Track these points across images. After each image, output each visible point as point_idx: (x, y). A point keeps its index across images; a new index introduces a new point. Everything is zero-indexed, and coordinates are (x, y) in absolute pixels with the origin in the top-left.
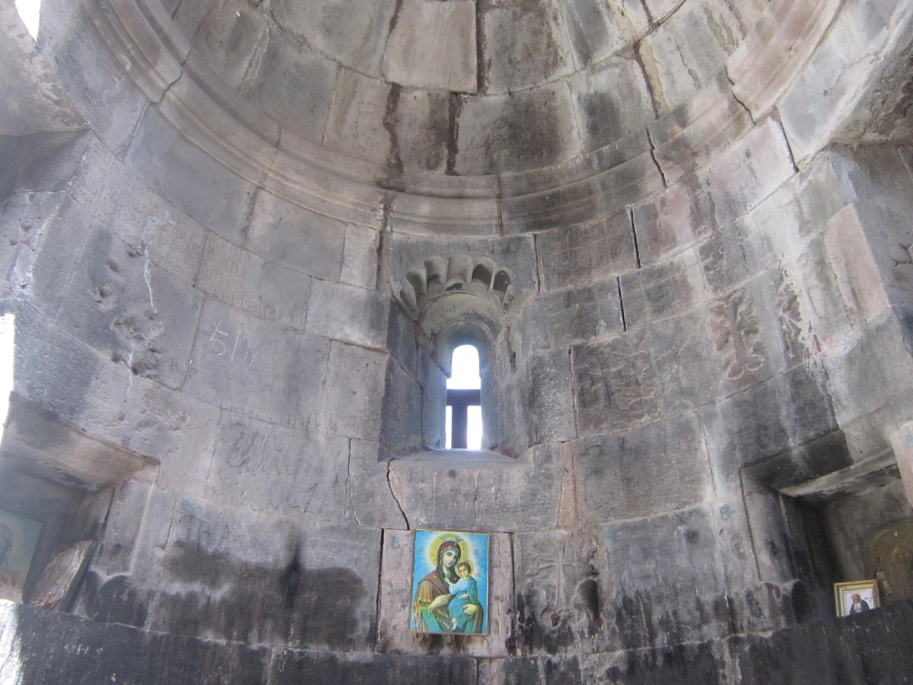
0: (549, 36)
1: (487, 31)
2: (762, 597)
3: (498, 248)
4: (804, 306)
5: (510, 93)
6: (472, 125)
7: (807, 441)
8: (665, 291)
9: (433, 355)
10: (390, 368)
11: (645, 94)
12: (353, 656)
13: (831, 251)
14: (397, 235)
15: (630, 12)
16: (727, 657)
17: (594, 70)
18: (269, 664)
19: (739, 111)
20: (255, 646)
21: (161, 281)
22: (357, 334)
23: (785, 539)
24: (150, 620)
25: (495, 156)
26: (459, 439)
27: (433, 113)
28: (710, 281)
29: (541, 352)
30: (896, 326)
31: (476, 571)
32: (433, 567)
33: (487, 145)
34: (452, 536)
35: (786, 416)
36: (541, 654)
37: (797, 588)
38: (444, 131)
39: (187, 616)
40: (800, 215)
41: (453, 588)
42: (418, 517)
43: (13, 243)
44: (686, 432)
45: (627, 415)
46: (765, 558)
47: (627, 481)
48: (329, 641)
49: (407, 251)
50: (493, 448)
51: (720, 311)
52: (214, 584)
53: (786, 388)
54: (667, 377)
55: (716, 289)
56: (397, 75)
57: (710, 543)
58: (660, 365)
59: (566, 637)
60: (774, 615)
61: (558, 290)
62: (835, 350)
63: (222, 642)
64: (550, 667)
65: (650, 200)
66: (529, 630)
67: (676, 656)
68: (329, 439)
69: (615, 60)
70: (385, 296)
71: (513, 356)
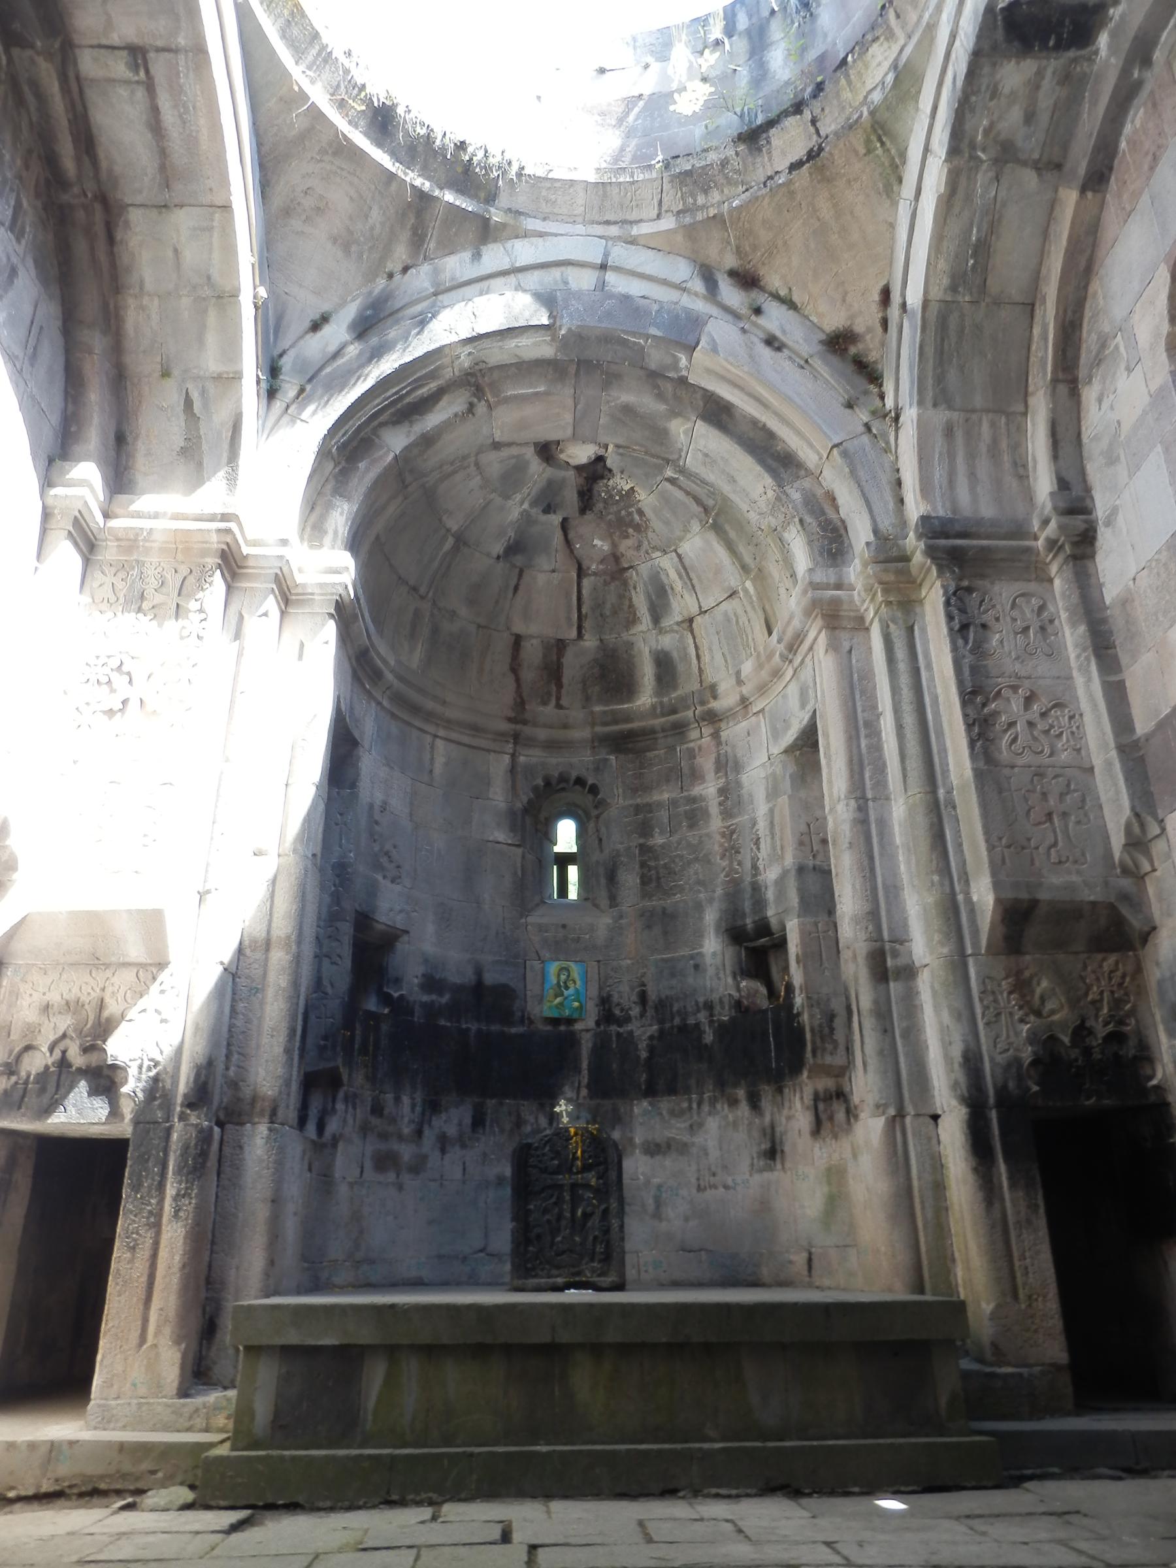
0: (630, 599)
1: (584, 592)
2: (726, 1000)
3: (591, 766)
4: (762, 846)
5: (601, 640)
6: (573, 666)
7: (754, 922)
8: (695, 815)
10: (523, 857)
11: (694, 661)
12: (514, 1030)
14: (522, 759)
15: (686, 596)
16: (707, 1029)
17: (661, 631)
19: (744, 702)
20: (464, 1026)
22: (500, 836)
24: (416, 1014)
25: (589, 691)
27: (545, 656)
28: (721, 813)
29: (620, 847)
30: (793, 872)
31: (578, 983)
32: (555, 982)
33: (584, 682)
34: (564, 964)
35: (747, 906)
36: (614, 1028)
38: (553, 672)
39: (431, 1011)
40: (767, 789)
41: (566, 993)
42: (546, 954)
43: (337, 824)
44: (699, 907)
46: (730, 980)
47: (665, 933)
50: (586, 899)
51: (723, 835)
52: (441, 994)
53: (749, 889)
54: (692, 871)
55: (723, 819)
56: (519, 627)
57: (705, 971)
58: (689, 863)
59: (628, 1019)
60: (730, 1009)
61: (631, 802)
62: (770, 875)
63: (448, 1024)
65: (691, 745)
66: (608, 1013)
67: (684, 1029)
69: (676, 628)
70: (519, 805)
71: (600, 840)
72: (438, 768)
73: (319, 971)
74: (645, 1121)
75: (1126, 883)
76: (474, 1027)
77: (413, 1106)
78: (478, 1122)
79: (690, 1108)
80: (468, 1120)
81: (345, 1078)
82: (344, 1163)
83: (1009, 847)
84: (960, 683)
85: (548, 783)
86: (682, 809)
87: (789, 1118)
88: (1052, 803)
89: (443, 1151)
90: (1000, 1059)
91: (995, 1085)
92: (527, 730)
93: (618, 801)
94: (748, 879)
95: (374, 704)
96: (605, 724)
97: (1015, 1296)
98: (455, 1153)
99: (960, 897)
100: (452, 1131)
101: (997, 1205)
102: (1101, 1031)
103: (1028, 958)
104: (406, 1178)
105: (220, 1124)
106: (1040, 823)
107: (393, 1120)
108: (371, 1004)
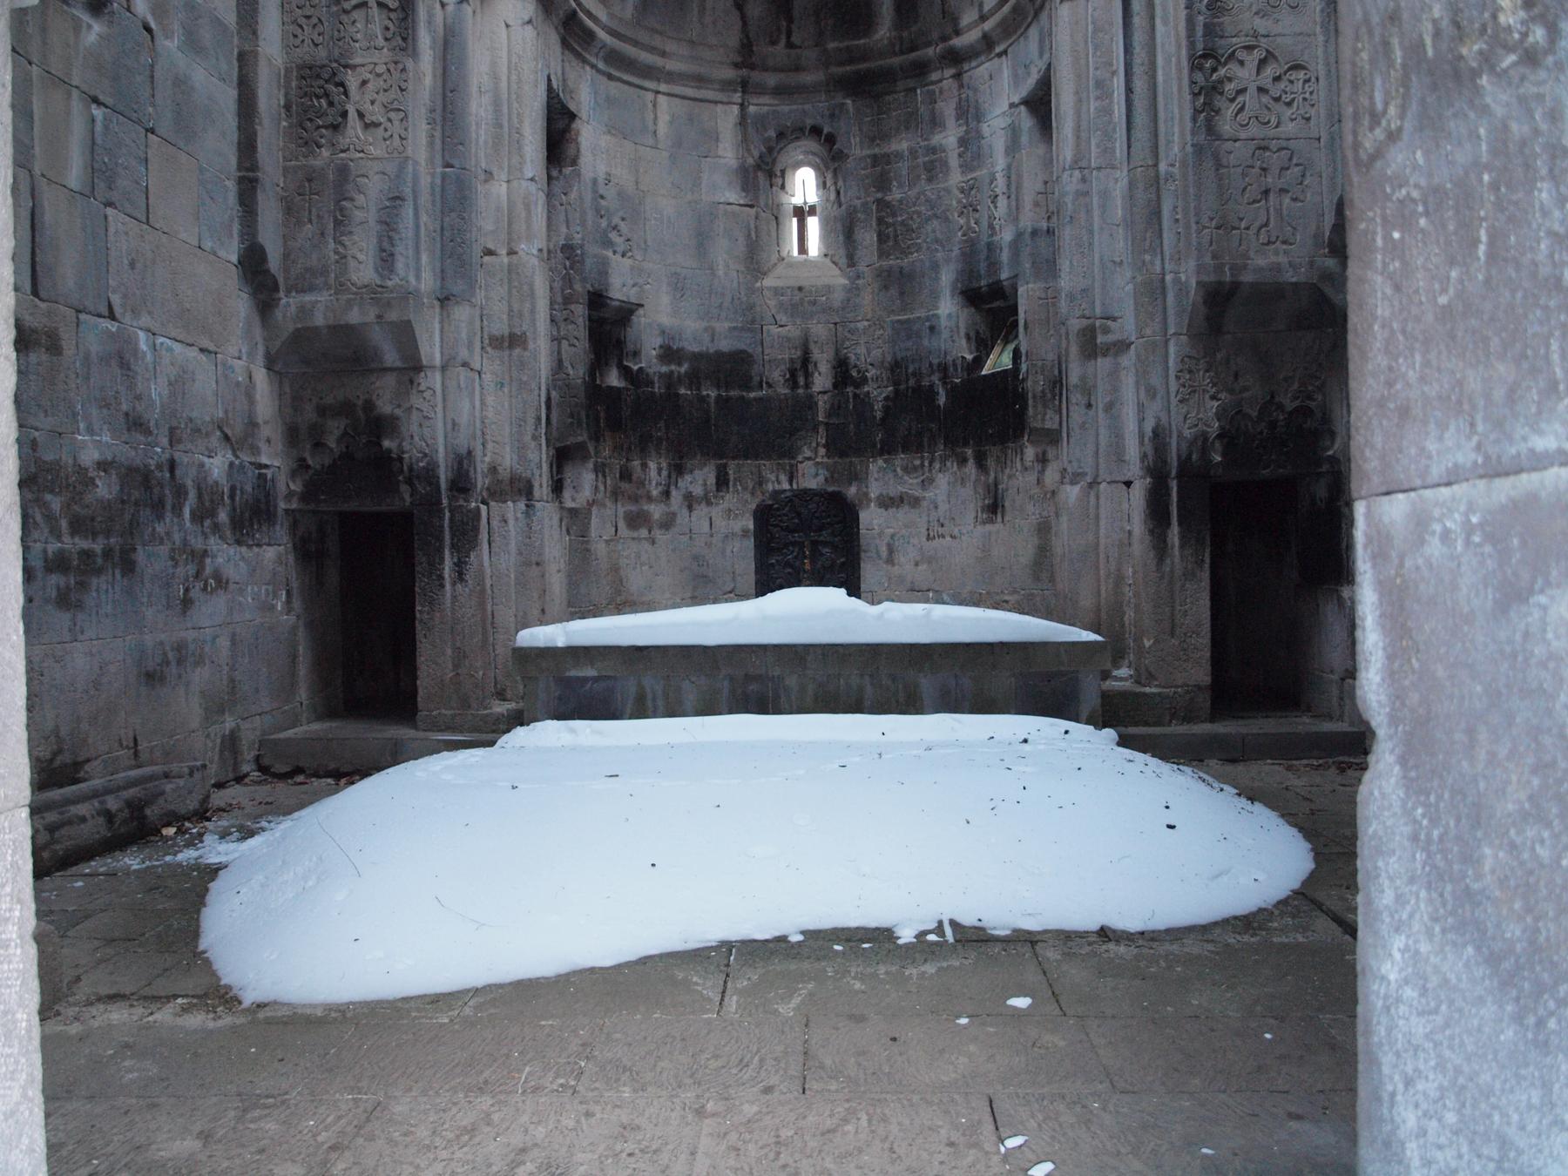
2: (959, 362)
8: (934, 167)
9: (783, 187)
12: (752, 395)
13: (1013, 177)
14: (752, 109)
18: (712, 400)
21: (621, 194)
22: (733, 196)
23: (978, 333)
29: (858, 203)
30: (1027, 236)
35: (983, 266)
37: (975, 359)
42: (782, 318)
44: (935, 267)
45: (905, 253)
46: (964, 342)
47: (902, 294)
48: (740, 387)
49: (761, 122)
52: (680, 364)
54: (929, 228)
57: (940, 333)
58: (928, 219)
59: (864, 380)
64: (856, 396)
67: (918, 389)
68: (726, 274)
70: (750, 161)
72: (662, 128)
73: (559, 353)
74: (879, 478)
75: (1331, 263)
76: (712, 393)
77: (660, 470)
78: (722, 482)
79: (922, 465)
80: (712, 480)
81: (591, 450)
82: (600, 526)
83: (1218, 228)
84: (1192, 44)
85: (781, 135)
86: (919, 160)
87: (1010, 477)
88: (1270, 180)
89: (690, 508)
90: (1187, 433)
91: (1179, 456)
92: (756, 76)
93: (857, 149)
94: (985, 239)
95: (588, 68)
96: (841, 64)
97: (1172, 634)
98: (701, 511)
99: (1168, 278)
100: (698, 490)
101: (1168, 561)
102: (1290, 405)
103: (1228, 337)
104: (657, 533)
106: (1255, 202)
107: (642, 484)
108: (614, 379)
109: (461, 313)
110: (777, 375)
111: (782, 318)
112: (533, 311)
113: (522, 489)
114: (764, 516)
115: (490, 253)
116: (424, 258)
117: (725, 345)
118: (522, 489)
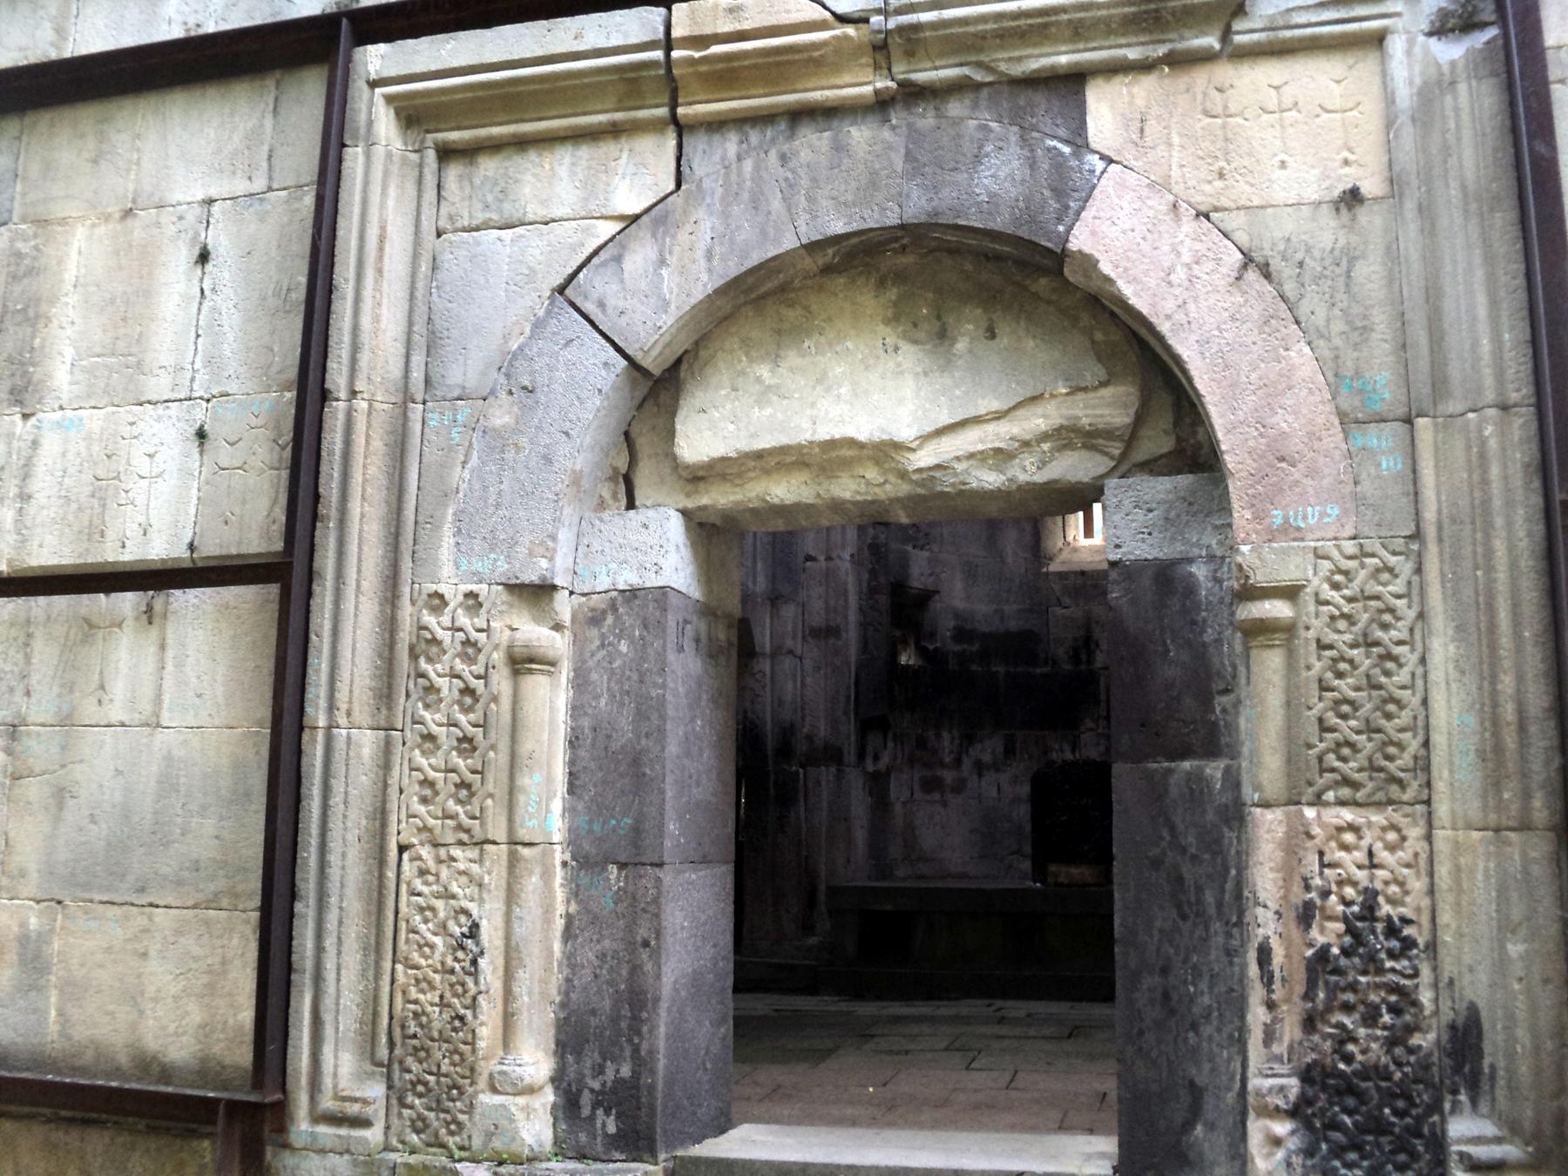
12: (1038, 671)
26: (1089, 532)
42: (1067, 601)
76: (1000, 669)
78: (1009, 751)
80: (1000, 749)
82: (897, 790)
89: (980, 775)
98: (990, 777)
100: (987, 758)
105: (802, 766)
109: (789, 611)
110: (1061, 652)
111: (1067, 601)
112: (846, 608)
113: (832, 755)
114: (1038, 782)
115: (809, 558)
116: (759, 565)
117: (1013, 625)
118: (832, 755)
